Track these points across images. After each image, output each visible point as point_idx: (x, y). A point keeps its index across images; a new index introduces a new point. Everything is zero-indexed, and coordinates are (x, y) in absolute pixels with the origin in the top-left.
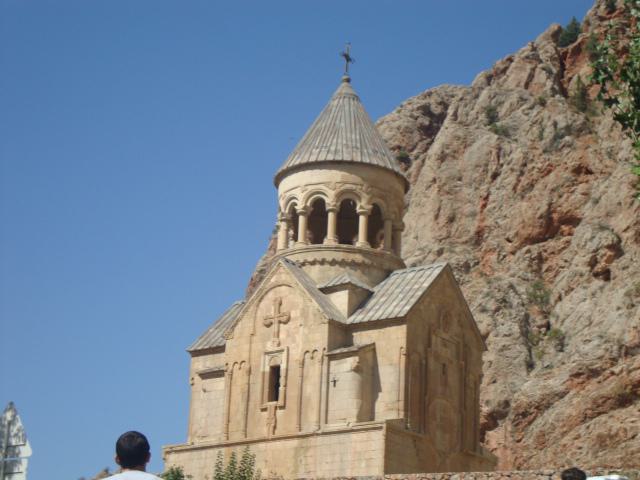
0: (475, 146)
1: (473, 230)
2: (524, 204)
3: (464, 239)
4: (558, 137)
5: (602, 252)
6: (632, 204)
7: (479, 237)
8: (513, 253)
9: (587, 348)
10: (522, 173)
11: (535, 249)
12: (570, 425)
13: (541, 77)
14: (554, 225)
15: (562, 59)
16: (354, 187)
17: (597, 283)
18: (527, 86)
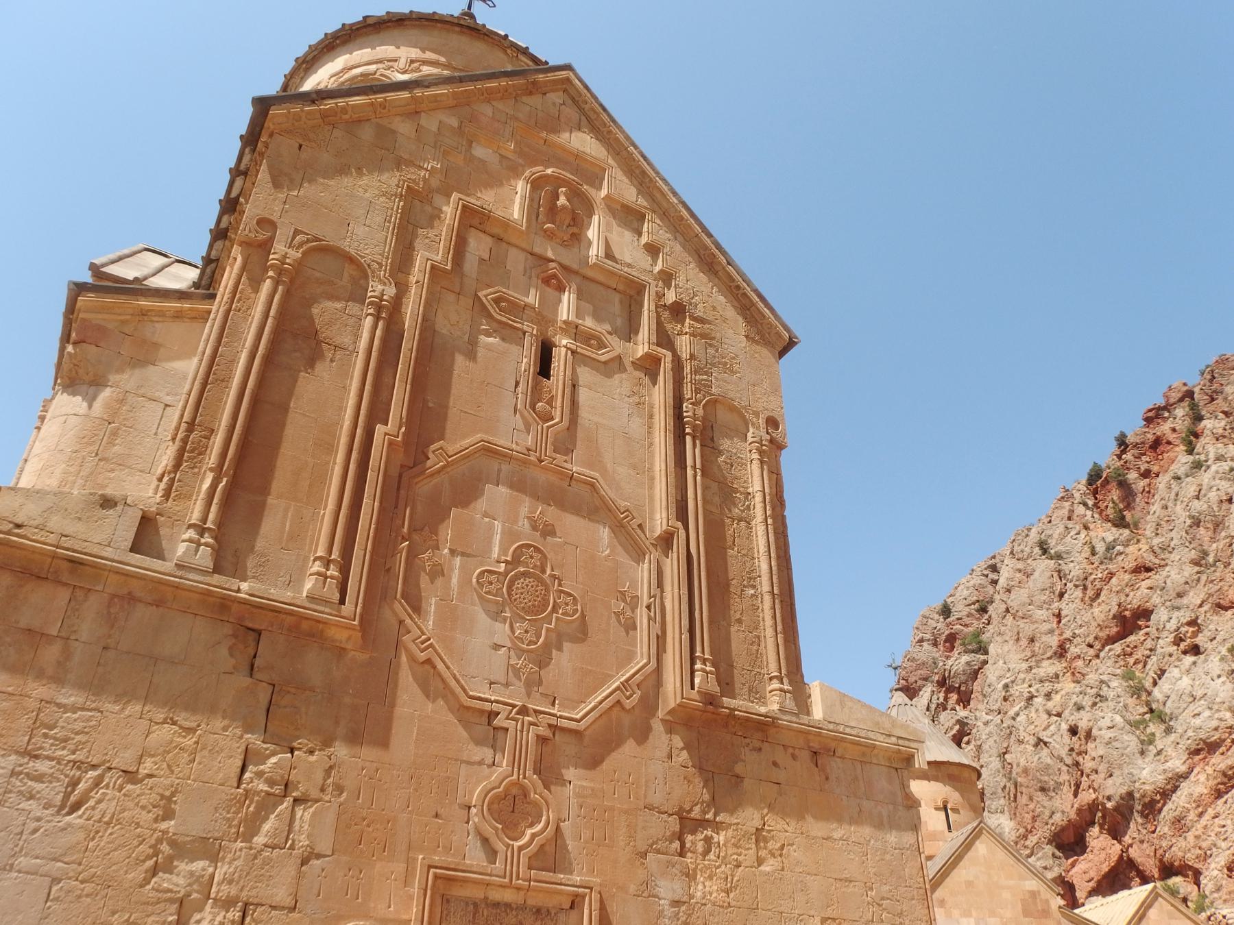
0: (1036, 574)
1: (1054, 641)
2: (1096, 610)
3: (1049, 654)
4: (1110, 548)
5: (1183, 630)
6: (1198, 580)
7: (1061, 652)
8: (1097, 656)
9: (1197, 722)
10: (1085, 588)
11: (1118, 647)
12: (1201, 806)
13: (1080, 510)
14: (1130, 622)
15: (1095, 492)
16: (373, 67)
17: (1189, 659)
18: (1069, 519)
